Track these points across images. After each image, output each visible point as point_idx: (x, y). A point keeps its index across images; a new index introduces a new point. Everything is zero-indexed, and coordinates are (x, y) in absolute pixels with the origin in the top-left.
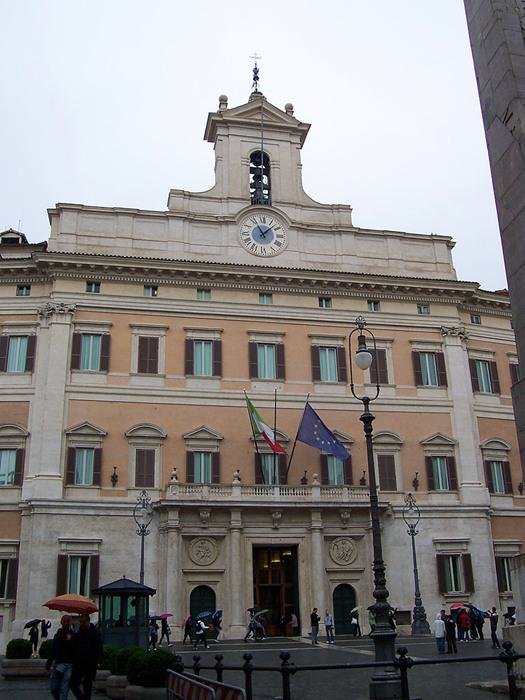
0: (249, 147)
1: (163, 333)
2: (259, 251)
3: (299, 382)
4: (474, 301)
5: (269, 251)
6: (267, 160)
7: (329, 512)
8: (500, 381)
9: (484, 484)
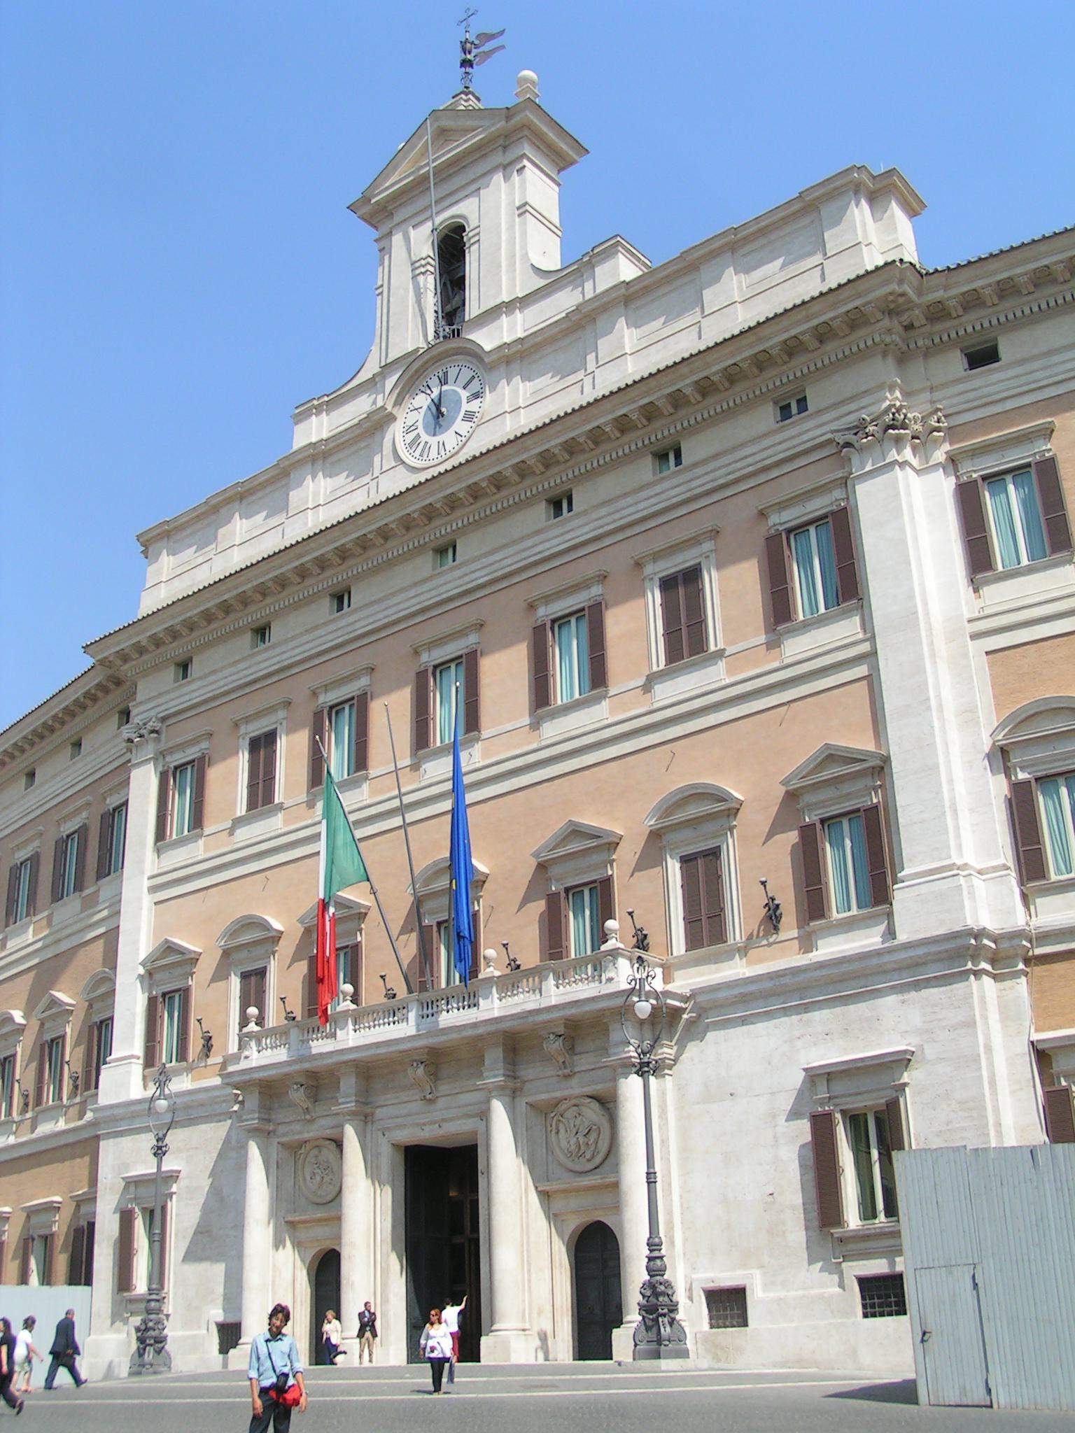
1: (281, 714)
4: (938, 313)
7: (516, 1042)
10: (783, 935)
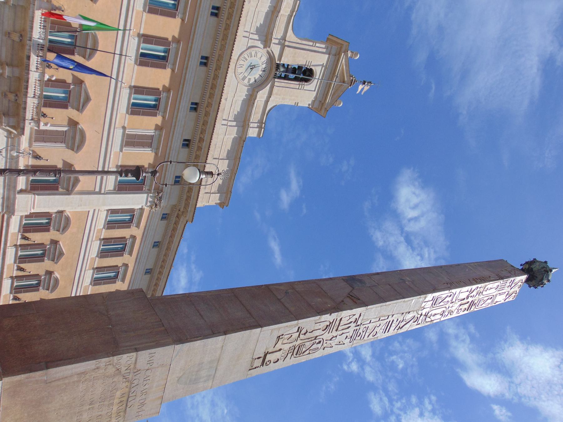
0: (318, 72)
2: (241, 62)
3: (134, 76)
5: (239, 70)
6: (306, 81)
8: (116, 230)
9: (33, 211)
10: (30, 159)
